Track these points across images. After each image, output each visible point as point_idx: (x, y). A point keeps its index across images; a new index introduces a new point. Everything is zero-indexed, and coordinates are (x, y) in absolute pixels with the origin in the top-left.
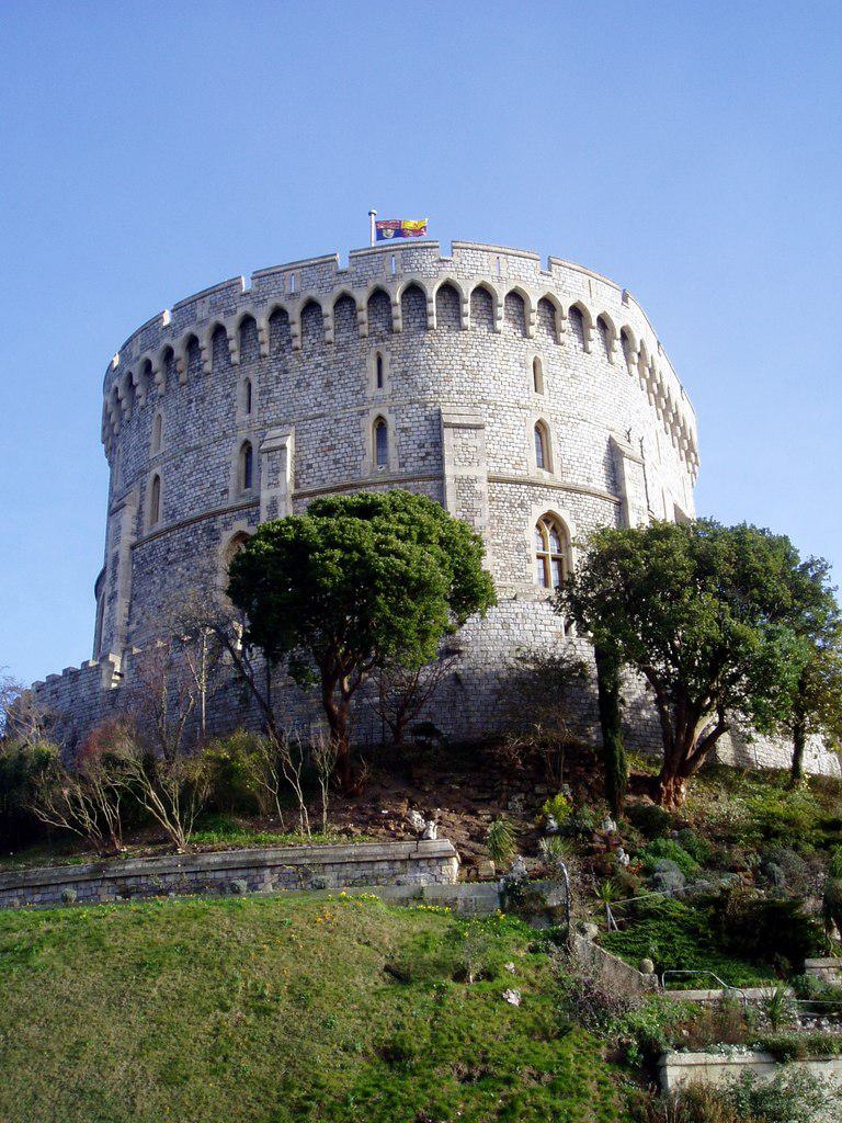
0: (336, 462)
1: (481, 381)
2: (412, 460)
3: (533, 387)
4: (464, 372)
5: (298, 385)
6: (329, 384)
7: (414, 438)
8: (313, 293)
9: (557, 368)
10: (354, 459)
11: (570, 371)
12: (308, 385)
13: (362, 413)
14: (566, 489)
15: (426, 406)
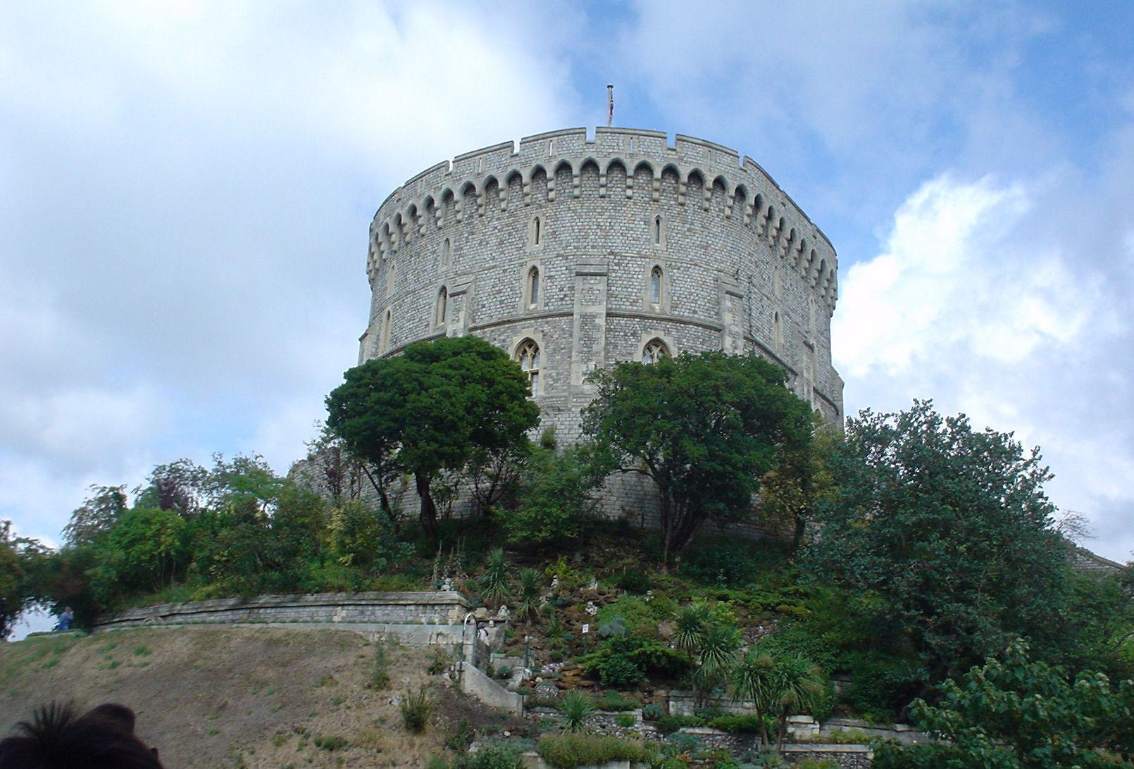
0: (502, 302)
1: (611, 237)
2: (553, 300)
3: (653, 240)
4: (598, 231)
5: (480, 244)
6: (501, 243)
7: (556, 283)
8: (494, 173)
9: (676, 224)
10: (513, 300)
11: (688, 226)
12: (487, 243)
13: (521, 265)
14: (671, 320)
15: (567, 259)
